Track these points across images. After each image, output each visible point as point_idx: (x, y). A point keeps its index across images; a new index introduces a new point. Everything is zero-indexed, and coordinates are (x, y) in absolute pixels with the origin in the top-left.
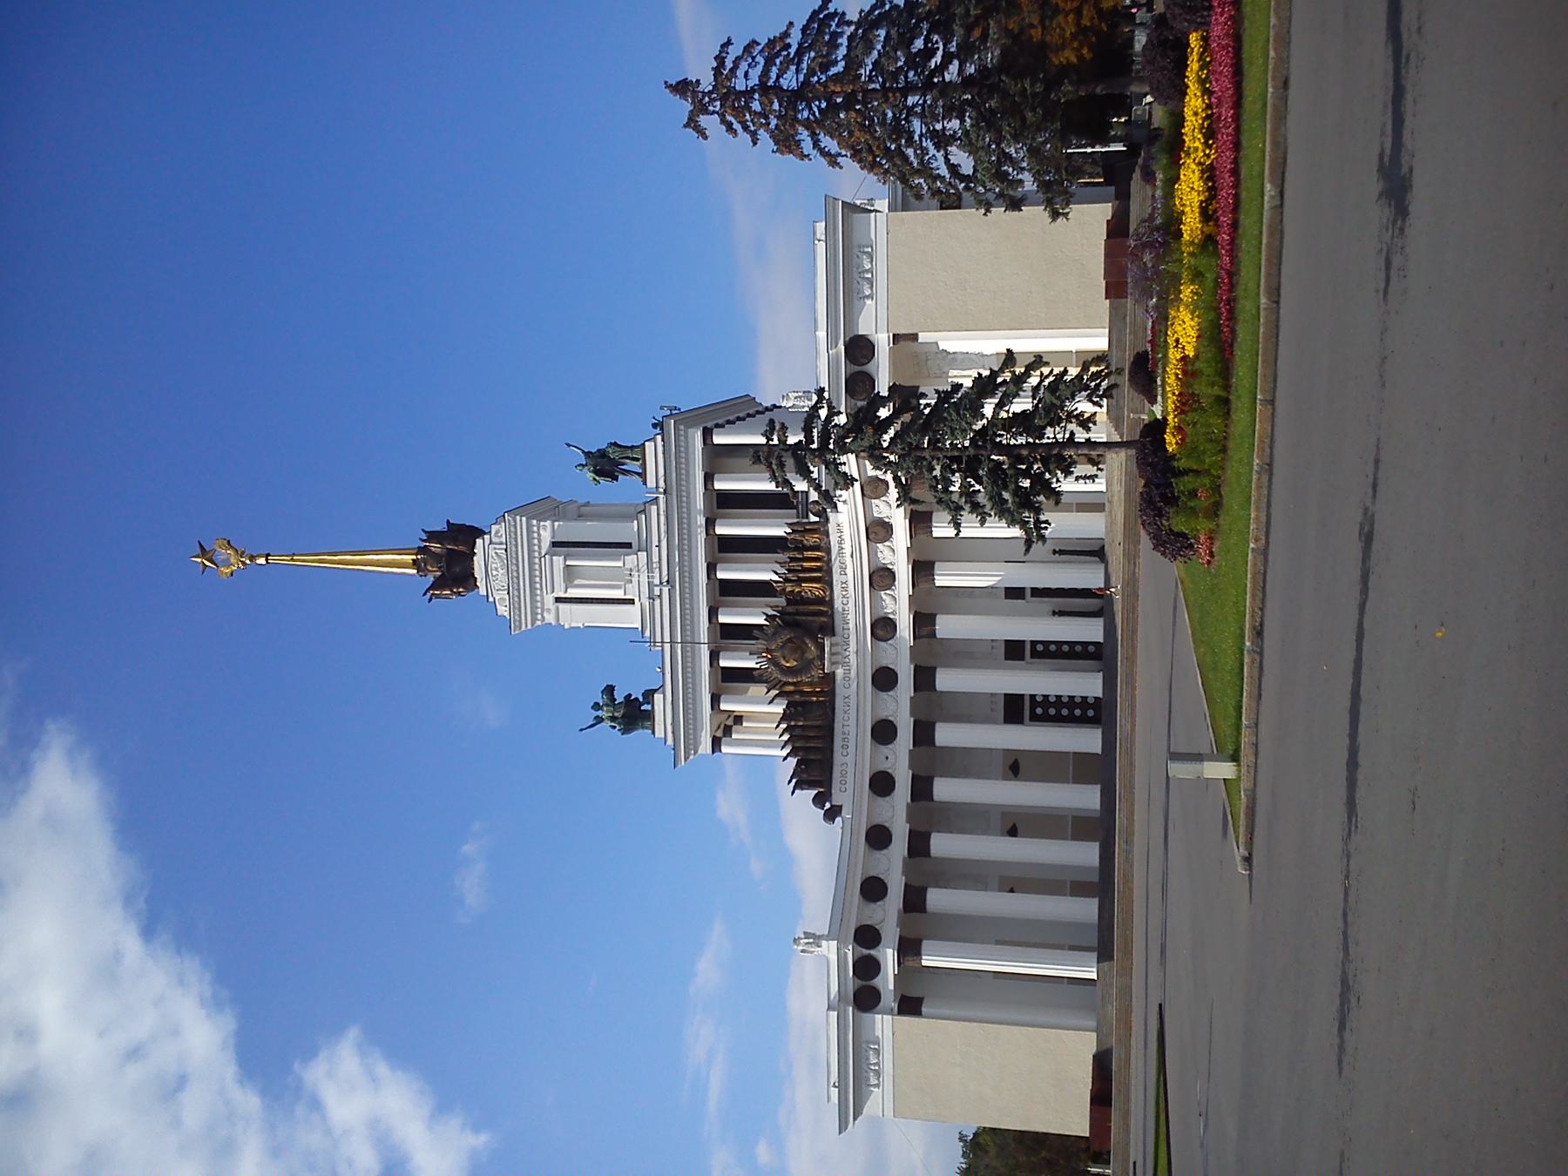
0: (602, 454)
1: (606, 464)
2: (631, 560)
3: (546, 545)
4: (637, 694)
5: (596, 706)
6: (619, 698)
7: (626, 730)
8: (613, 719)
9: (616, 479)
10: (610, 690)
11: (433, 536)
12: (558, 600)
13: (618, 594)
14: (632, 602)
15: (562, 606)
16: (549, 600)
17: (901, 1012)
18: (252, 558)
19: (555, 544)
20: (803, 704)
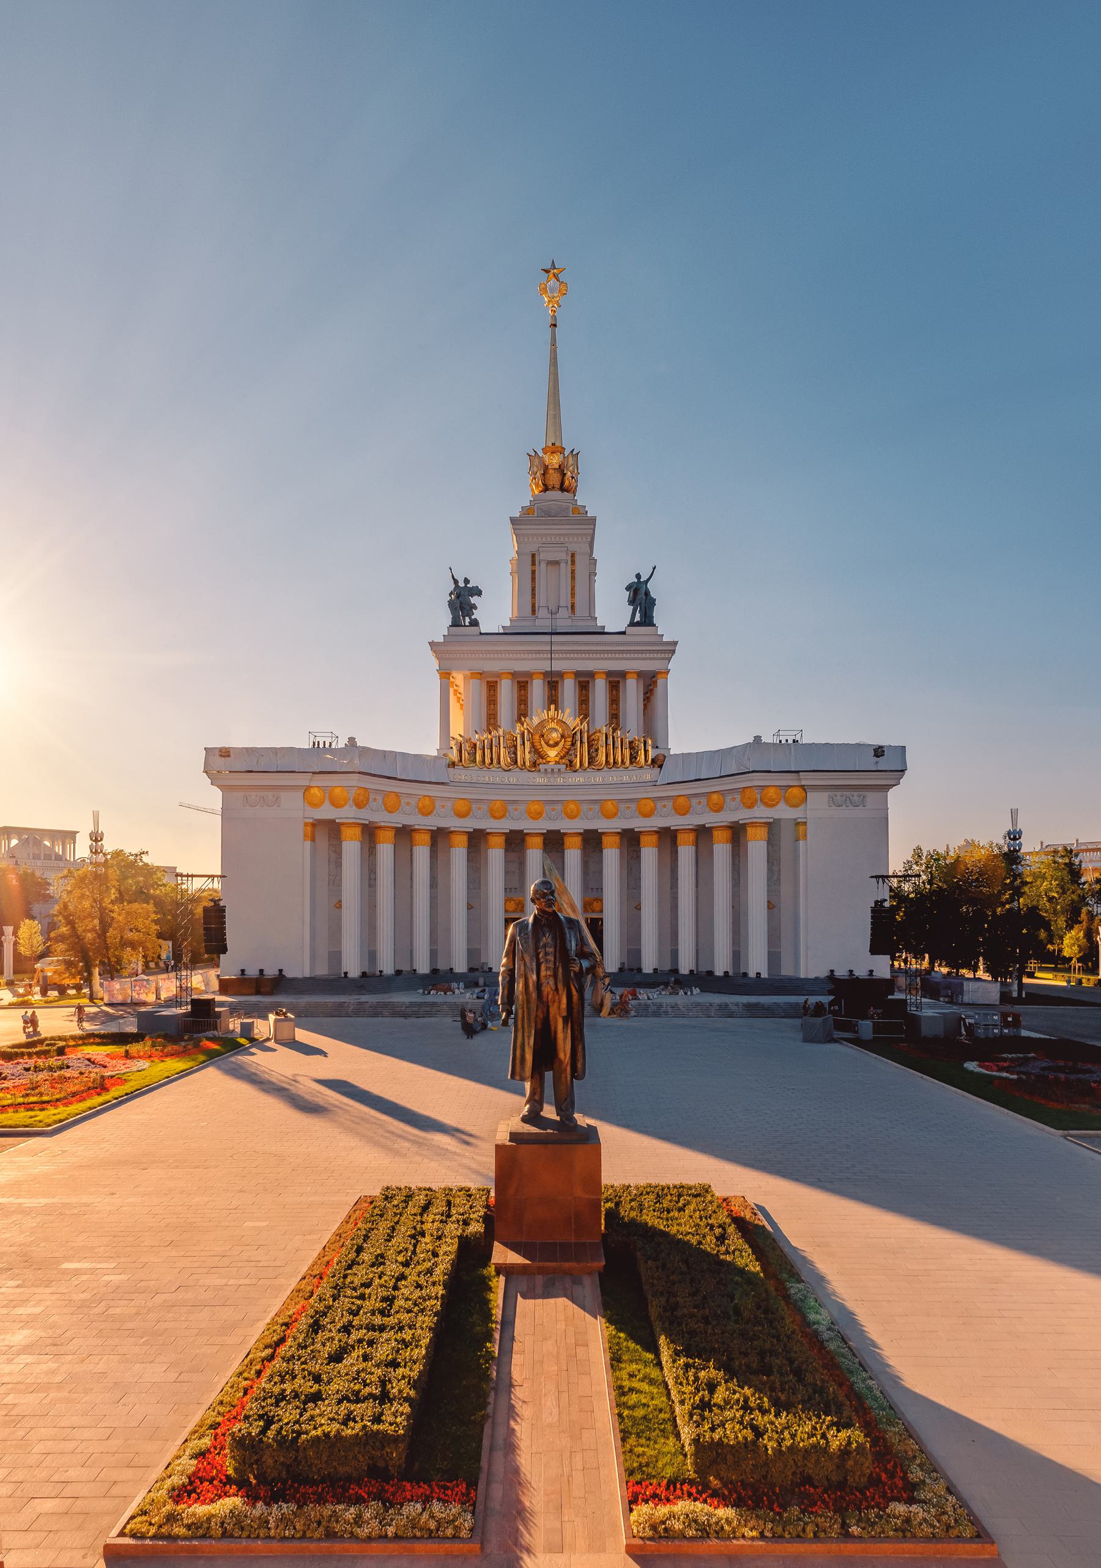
0: (647, 593)
1: (641, 598)
2: (564, 613)
3: (573, 547)
4: (476, 615)
5: (467, 581)
6: (474, 600)
7: (451, 604)
8: (458, 596)
9: (632, 602)
10: (478, 592)
12: (533, 556)
13: (541, 599)
14: (534, 611)
15: (529, 558)
16: (533, 548)
17: (306, 824)
20: (515, 747)
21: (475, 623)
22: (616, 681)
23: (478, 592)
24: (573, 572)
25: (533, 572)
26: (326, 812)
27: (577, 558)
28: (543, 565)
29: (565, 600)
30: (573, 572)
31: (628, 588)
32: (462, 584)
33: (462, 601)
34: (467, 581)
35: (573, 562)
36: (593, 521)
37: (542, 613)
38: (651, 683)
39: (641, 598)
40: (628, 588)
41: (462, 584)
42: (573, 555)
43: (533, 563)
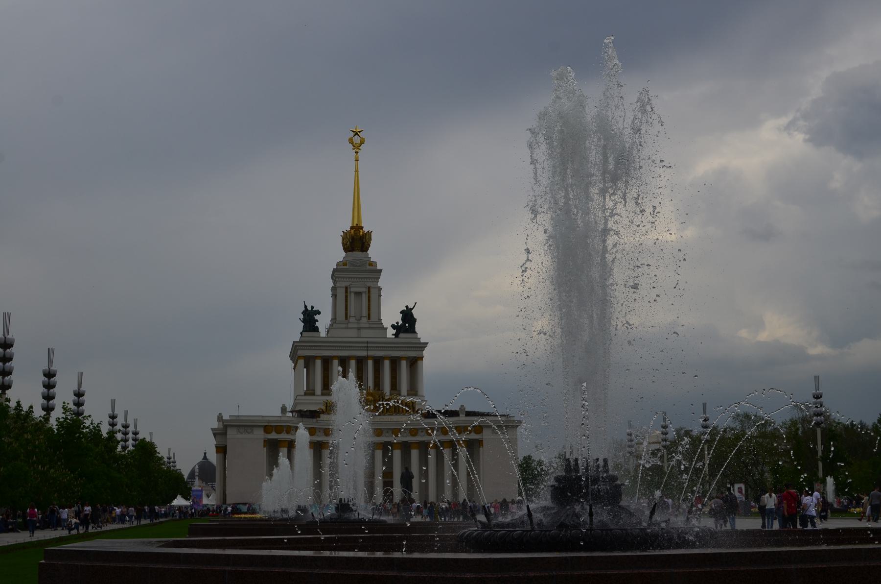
0: (412, 315)
1: (408, 316)
2: (364, 320)
3: (369, 284)
4: (317, 324)
5: (312, 307)
6: (317, 317)
7: (304, 321)
10: (319, 313)
11: (369, 233)
14: (346, 318)
16: (347, 284)
18: (357, 153)
19: (369, 288)
21: (316, 330)
22: (395, 363)
23: (319, 313)
24: (369, 297)
25: (346, 297)
26: (273, 436)
27: (372, 290)
28: (353, 295)
29: (365, 313)
30: (369, 297)
31: (401, 312)
32: (309, 309)
33: (309, 318)
34: (312, 307)
35: (369, 292)
36: (380, 271)
37: (352, 320)
38: (414, 363)
39: (408, 316)
40: (401, 312)
41: (309, 309)
42: (369, 288)
43: (346, 292)
